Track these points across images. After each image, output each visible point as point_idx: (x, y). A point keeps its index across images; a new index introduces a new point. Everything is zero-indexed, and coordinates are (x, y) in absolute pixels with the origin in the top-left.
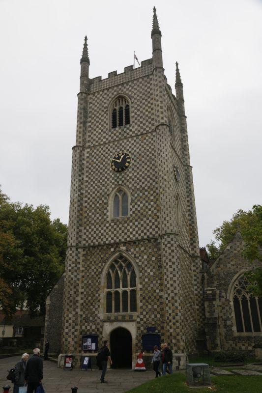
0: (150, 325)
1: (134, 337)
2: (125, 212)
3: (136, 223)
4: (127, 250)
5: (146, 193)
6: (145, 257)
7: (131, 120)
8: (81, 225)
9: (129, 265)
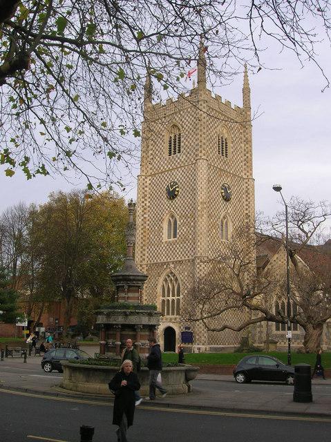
0: (187, 326)
1: (177, 333)
2: (175, 236)
3: (181, 245)
4: (175, 268)
5: (189, 220)
6: (186, 273)
7: (182, 149)
8: (144, 245)
9: (176, 280)
